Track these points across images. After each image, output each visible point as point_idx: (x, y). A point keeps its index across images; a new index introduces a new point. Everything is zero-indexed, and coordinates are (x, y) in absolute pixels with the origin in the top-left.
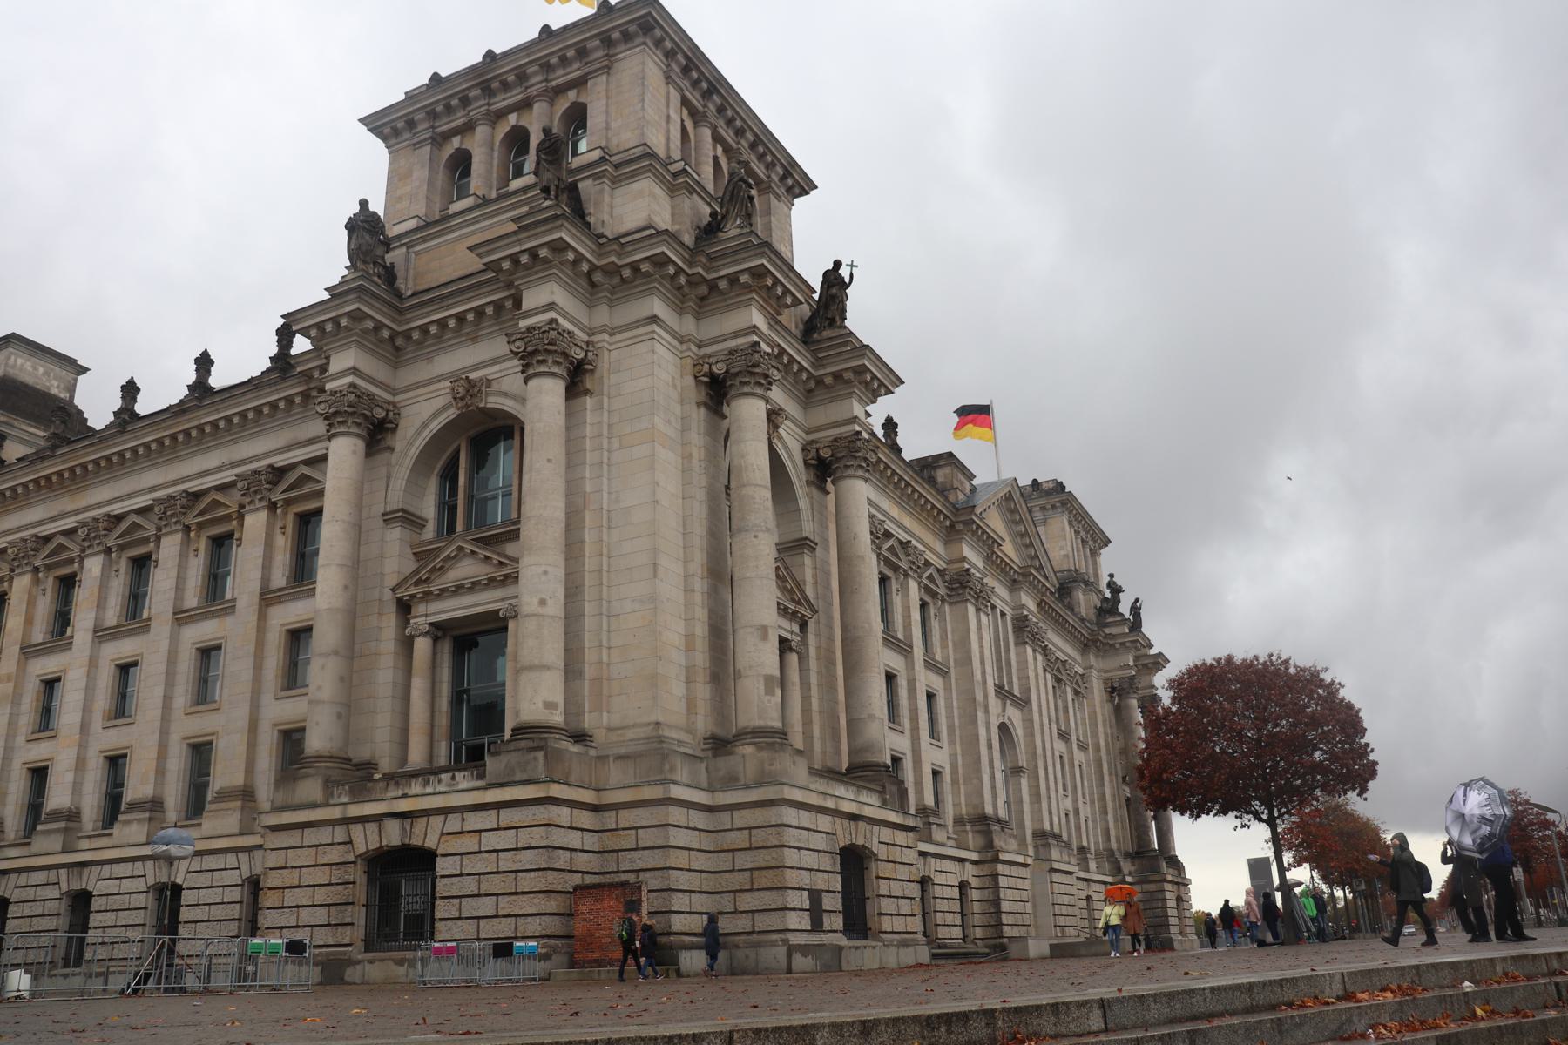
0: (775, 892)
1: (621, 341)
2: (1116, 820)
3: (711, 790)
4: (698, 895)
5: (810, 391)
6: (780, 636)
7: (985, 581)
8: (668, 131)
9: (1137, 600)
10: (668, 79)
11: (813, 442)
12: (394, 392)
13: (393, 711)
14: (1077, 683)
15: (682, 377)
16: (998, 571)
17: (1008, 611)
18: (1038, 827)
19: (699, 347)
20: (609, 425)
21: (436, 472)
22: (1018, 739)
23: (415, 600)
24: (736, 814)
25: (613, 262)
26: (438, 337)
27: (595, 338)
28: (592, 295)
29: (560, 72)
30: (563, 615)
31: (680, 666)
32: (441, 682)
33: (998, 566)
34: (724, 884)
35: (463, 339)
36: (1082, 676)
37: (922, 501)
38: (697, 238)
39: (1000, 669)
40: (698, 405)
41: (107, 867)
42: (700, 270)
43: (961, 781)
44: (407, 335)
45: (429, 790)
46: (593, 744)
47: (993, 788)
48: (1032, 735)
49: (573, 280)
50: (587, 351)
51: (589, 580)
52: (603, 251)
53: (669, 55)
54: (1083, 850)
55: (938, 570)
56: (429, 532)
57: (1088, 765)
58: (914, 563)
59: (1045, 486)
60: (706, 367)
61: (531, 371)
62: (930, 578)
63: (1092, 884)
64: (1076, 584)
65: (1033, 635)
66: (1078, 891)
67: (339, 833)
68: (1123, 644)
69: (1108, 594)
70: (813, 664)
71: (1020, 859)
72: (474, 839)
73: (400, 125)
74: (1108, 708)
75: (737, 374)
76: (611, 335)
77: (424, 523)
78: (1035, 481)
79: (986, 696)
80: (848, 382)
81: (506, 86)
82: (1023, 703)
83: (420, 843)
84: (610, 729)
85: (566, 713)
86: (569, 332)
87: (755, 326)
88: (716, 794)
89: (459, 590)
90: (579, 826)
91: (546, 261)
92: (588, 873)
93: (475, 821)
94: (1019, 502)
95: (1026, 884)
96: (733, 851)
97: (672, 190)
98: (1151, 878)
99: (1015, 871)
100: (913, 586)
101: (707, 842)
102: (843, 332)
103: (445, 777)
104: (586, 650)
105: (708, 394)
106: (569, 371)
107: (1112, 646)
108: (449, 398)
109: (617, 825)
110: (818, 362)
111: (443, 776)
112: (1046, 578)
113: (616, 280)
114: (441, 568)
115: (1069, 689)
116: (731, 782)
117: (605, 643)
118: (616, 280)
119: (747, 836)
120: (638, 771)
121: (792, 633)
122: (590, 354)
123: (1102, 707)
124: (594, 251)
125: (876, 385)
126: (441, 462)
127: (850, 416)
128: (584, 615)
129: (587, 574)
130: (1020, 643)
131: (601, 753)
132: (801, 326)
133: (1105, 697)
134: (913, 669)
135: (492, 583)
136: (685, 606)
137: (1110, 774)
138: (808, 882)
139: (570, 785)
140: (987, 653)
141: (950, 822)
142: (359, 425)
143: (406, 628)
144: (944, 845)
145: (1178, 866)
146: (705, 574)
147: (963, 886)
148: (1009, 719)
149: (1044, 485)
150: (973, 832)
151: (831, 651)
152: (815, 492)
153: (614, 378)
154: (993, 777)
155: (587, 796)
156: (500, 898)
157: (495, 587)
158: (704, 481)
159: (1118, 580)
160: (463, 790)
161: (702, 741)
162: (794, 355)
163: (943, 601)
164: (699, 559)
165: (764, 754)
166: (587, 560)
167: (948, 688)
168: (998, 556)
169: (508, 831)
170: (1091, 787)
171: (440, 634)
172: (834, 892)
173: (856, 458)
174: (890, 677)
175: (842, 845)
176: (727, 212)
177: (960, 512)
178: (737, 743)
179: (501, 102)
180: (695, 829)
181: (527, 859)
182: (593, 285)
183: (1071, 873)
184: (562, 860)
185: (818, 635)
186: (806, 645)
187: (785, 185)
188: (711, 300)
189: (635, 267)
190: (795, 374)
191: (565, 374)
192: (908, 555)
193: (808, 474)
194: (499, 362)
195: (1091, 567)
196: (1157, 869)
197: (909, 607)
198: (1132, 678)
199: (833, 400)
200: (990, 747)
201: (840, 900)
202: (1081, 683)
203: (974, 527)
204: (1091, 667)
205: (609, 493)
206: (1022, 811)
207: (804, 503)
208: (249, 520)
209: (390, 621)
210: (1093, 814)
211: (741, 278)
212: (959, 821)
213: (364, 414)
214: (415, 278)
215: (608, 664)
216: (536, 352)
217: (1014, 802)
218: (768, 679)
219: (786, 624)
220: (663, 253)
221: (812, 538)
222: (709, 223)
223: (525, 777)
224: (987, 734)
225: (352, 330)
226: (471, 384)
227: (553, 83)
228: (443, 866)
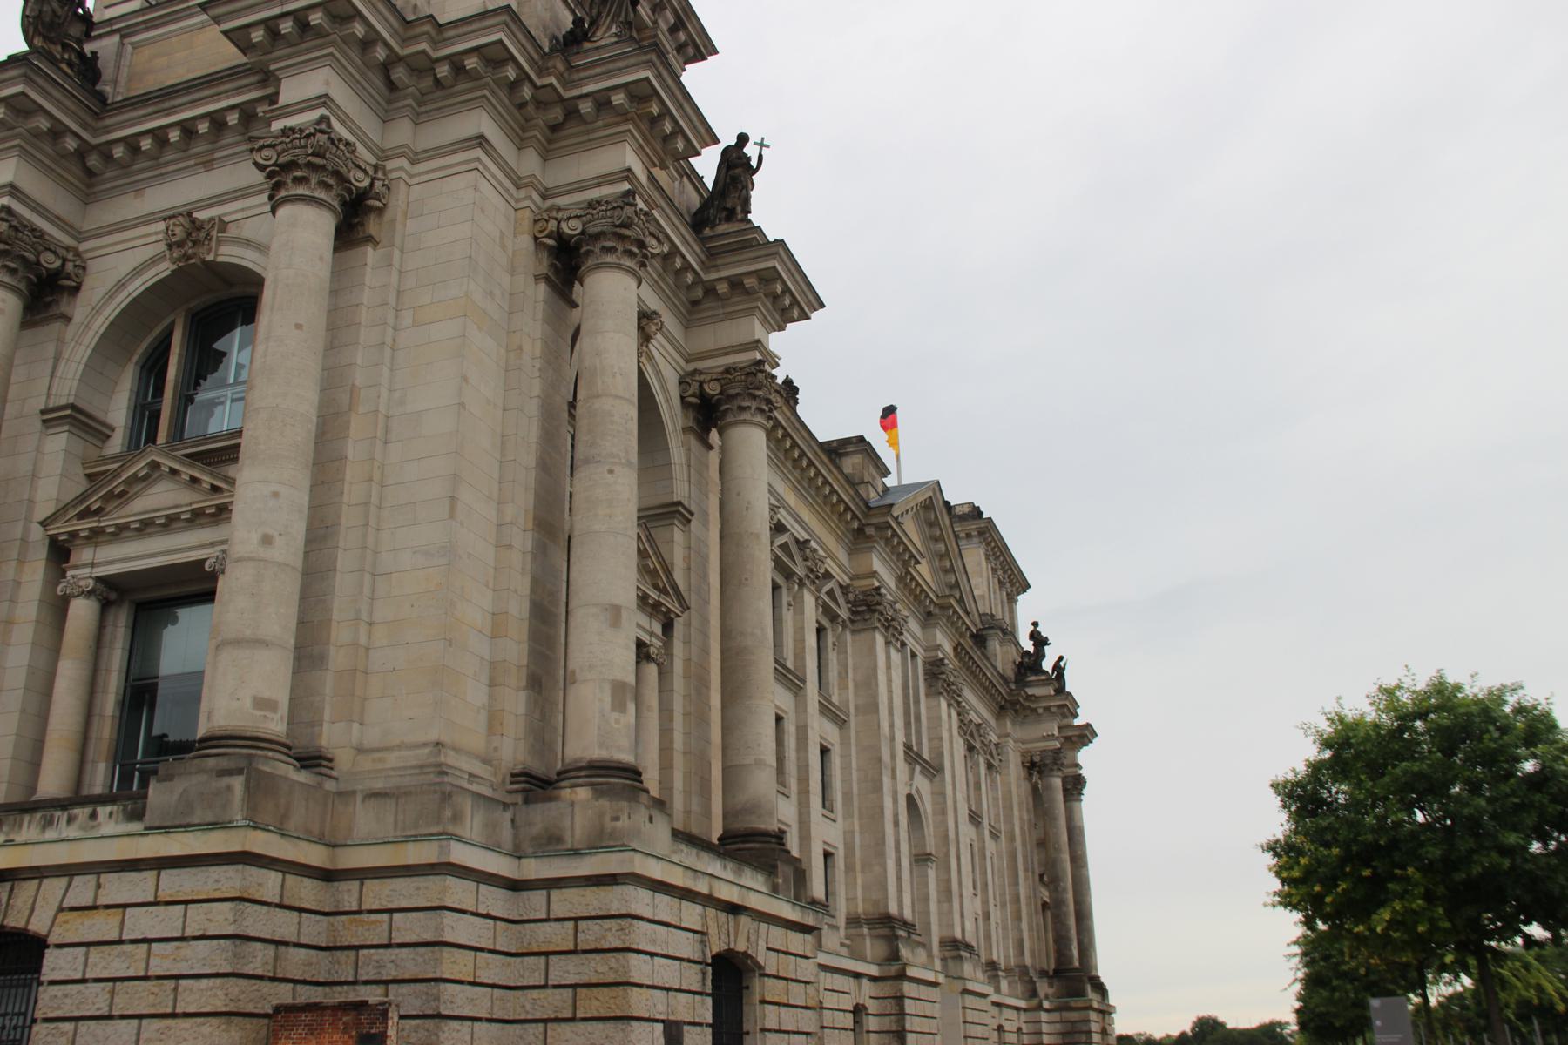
0: (610, 1025)
1: (427, 172)
2: (1030, 929)
3: (518, 854)
4: (486, 1025)
5: (695, 303)
6: (638, 639)
7: (898, 606)
9: (1061, 658)
11: (695, 372)
12: (80, 236)
13: (23, 711)
14: (991, 754)
15: (515, 236)
16: (911, 598)
17: (920, 652)
18: (946, 933)
19: (544, 198)
20: (399, 292)
21: (135, 358)
22: (926, 818)
23: (78, 542)
24: (555, 894)
25: (423, 52)
26: (154, 157)
27: (390, 165)
28: (389, 102)
30: (299, 564)
31: (482, 658)
32: (108, 671)
33: (911, 591)
34: (528, 1007)
35: (192, 162)
36: (997, 745)
37: (827, 490)
40: (537, 278)
42: (553, 80)
43: (858, 867)
44: (105, 152)
45: (51, 834)
46: (334, 773)
47: (899, 878)
48: (944, 812)
49: (362, 74)
50: (373, 179)
51: (349, 519)
52: (411, 33)
54: (992, 966)
55: (841, 586)
56: (116, 444)
57: (1000, 858)
58: (812, 571)
59: (958, 511)
60: (552, 225)
61: (283, 193)
62: (830, 593)
63: (1004, 1010)
64: (991, 632)
65: (948, 685)
66: (992, 1018)
68: (1047, 709)
69: (1028, 646)
70: (678, 683)
71: (930, 976)
72: (114, 917)
74: (1026, 787)
75: (597, 237)
76: (413, 163)
77: (107, 432)
79: (893, 757)
80: (748, 292)
82: (933, 770)
83: (21, 924)
84: (360, 750)
85: (291, 721)
86: (347, 144)
87: (629, 170)
88: (524, 861)
89: (146, 527)
90: (297, 904)
91: (319, 33)
92: (304, 982)
93: (119, 888)
94: (941, 513)
95: (935, 1010)
96: (547, 954)
98: (1073, 1004)
99: (925, 992)
100: (809, 600)
101: (505, 938)
102: (744, 226)
103: (82, 813)
104: (334, 624)
105: (552, 265)
106: (344, 204)
107: (1034, 710)
108: (162, 247)
109: (360, 905)
110: (712, 256)
111: (77, 811)
112: (968, 613)
113: (428, 82)
114: (122, 494)
115: (982, 761)
116: (550, 843)
117: (364, 616)
118: (428, 82)
119: (571, 932)
120: (401, 817)
121: (652, 634)
122: (378, 184)
123: (1018, 786)
124: (395, 31)
125: (787, 301)
126: (144, 345)
127: (748, 339)
128: (335, 570)
129: (345, 508)
130: (932, 692)
131: (343, 787)
133: (1022, 773)
134: (805, 711)
135: (197, 517)
136: (495, 569)
137: (1026, 870)
138: (662, 1008)
139: (283, 835)
142: (13, 272)
143: (57, 585)
144: (836, 954)
145: (1101, 989)
146: (530, 525)
147: (858, 1011)
148: (918, 790)
149: (958, 509)
150: (872, 937)
151: (704, 668)
152: (693, 442)
153: (412, 226)
155: (314, 855)
156: (145, 1022)
157: (202, 526)
158: (537, 388)
159: (1044, 631)
160: (102, 837)
161: (508, 779)
162: (679, 244)
163: (844, 626)
164: (521, 505)
165: (604, 803)
166: (346, 486)
167: (845, 741)
168: (913, 578)
169: (170, 908)
171: (113, 596)
172: (700, 1024)
173: (754, 397)
175: (715, 950)
176: (599, 14)
177: (871, 513)
178: (563, 784)
180: (488, 916)
181: (198, 956)
182: (392, 86)
183: (984, 996)
184: (259, 959)
185: (687, 641)
186: (670, 655)
187: (676, 39)
188: (566, 132)
189: (456, 62)
190: (678, 273)
191: (336, 204)
192: (806, 559)
193: (686, 416)
194: (243, 197)
195: (1007, 614)
196: (1080, 993)
197: (802, 628)
198: (1057, 752)
199: (728, 317)
200: (896, 824)
201: (710, 1038)
202: (995, 756)
203: (889, 533)
204: (1008, 735)
205: (390, 391)
206: (928, 913)
207: (677, 455)
211: (613, 98)
213: (23, 258)
214: (130, 80)
215: (368, 649)
216: (292, 165)
218: (618, 688)
219: (644, 620)
220: (500, 42)
221: (686, 504)
222: (571, 32)
223: (210, 819)
224: (892, 807)
225: (13, 128)
226: (196, 226)
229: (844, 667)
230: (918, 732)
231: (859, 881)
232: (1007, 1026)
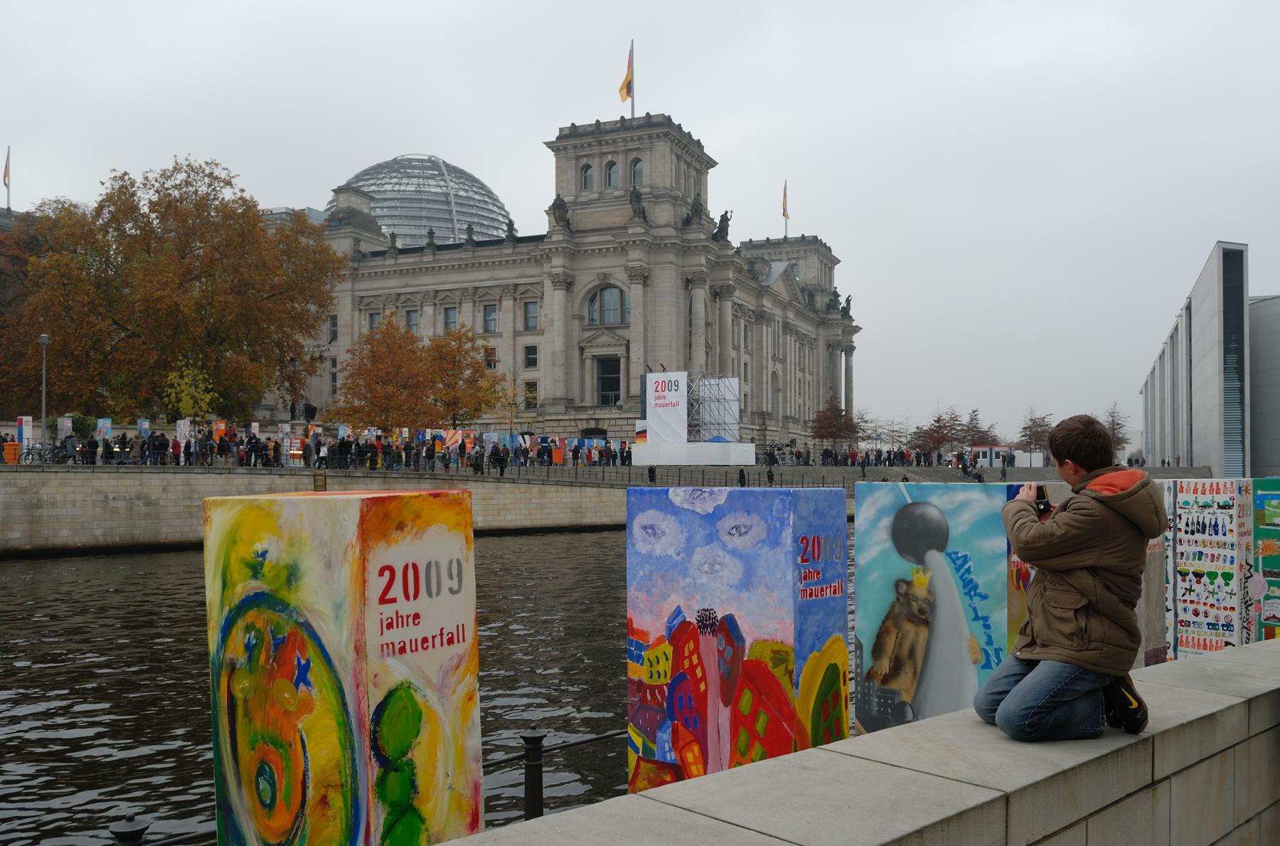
10: (672, 150)
12: (572, 270)
17: (781, 320)
29: (630, 144)
39: (774, 347)
44: (579, 251)
56: (586, 321)
57: (813, 381)
67: (573, 423)
71: (775, 429)
73: (561, 148)
78: (803, 235)
81: (607, 143)
82: (784, 361)
93: (619, 422)
97: (674, 205)
99: (773, 433)
100: (742, 321)
112: (799, 303)
130: (785, 333)
140: (770, 344)
141: (749, 414)
167: (752, 360)
170: (813, 392)
189: (665, 244)
198: (839, 341)
209: (577, 353)
210: (813, 405)
212: (752, 413)
217: (775, 404)
224: (766, 378)
227: (628, 148)
232: (809, 443)
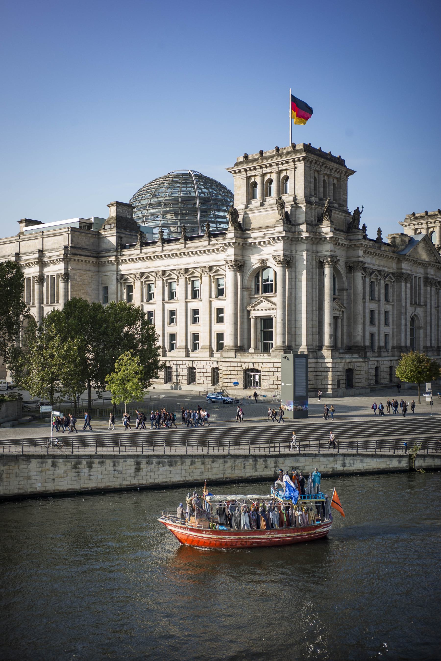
8: (310, 186)
17: (422, 276)
38: (317, 221)
39: (415, 297)
41: (175, 362)
43: (395, 336)
45: (258, 357)
53: (311, 162)
60: (318, 259)
62: (390, 277)
70: (345, 321)
81: (266, 167)
93: (269, 365)
100: (382, 282)
113: (297, 240)
130: (426, 286)
132: (347, 226)
148: (417, 313)
154: (406, 334)
167: (393, 309)
174: (372, 312)
179: (265, 171)
206: (420, 341)
207: (345, 279)
208: (204, 278)
212: (393, 348)
228: (262, 373)
229: (394, 291)
230: (420, 297)
231: (395, 339)
